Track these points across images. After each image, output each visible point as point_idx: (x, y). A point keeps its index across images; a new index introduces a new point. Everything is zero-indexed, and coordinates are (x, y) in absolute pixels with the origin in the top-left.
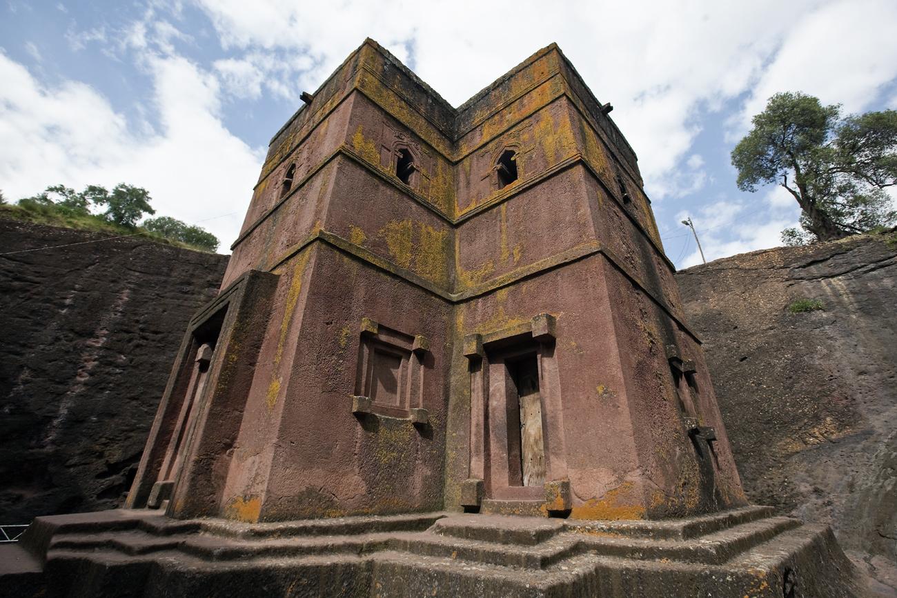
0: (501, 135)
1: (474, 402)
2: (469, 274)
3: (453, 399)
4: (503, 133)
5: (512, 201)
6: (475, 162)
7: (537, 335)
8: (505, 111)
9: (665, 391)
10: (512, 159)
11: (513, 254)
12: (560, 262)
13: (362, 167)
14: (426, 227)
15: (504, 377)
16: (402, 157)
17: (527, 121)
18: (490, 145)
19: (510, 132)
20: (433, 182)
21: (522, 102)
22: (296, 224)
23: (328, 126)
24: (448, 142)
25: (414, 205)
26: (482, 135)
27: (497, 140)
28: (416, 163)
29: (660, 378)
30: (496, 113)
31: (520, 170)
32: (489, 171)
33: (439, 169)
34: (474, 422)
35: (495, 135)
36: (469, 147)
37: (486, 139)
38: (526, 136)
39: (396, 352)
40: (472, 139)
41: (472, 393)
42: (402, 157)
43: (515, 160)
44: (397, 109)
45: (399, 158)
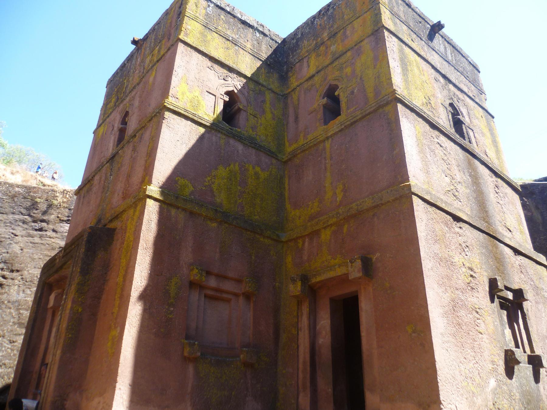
1: (301, 341)
2: (297, 212)
3: (284, 337)
7: (353, 277)
9: (483, 325)
10: (336, 93)
11: (336, 193)
13: (187, 118)
14: (254, 168)
15: (329, 315)
17: (349, 54)
18: (316, 78)
21: (345, 33)
22: (129, 176)
23: (155, 75)
25: (240, 147)
29: (477, 312)
30: (322, 44)
31: (343, 105)
34: (301, 360)
37: (312, 71)
38: (348, 70)
39: (225, 296)
41: (300, 332)
43: (339, 95)
45: (225, 101)
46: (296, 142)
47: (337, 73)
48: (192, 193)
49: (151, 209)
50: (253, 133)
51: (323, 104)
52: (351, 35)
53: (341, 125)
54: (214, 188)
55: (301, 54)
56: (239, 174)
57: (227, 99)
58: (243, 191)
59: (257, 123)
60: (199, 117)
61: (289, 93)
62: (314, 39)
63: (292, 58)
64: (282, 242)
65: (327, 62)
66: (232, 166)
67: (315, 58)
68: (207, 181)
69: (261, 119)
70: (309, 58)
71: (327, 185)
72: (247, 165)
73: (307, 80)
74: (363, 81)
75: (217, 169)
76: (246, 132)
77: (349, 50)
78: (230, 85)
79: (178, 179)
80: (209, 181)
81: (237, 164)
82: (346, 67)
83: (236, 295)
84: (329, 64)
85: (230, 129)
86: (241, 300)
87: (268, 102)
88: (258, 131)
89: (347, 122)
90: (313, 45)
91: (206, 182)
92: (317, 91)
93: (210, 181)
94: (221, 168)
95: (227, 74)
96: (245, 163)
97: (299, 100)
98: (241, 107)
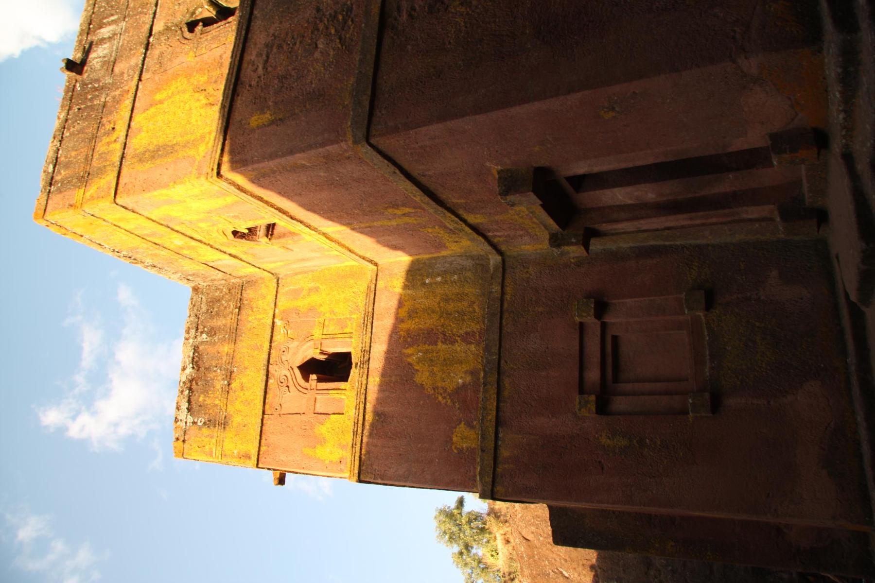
12: (403, 178)
28: (311, 352)
48: (470, 425)
49: (509, 489)
50: (350, 325)
54: (451, 387)
56: (418, 346)
57: (313, 377)
58: (442, 336)
59: (333, 319)
60: (356, 425)
64: (503, 261)
68: (445, 400)
69: (324, 313)
71: (395, 224)
75: (422, 385)
79: (456, 448)
80: (444, 398)
83: (604, 326)
85: (356, 367)
86: (609, 319)
91: (447, 402)
93: (443, 395)
94: (418, 379)
95: (279, 381)
96: (400, 338)
98: (318, 351)
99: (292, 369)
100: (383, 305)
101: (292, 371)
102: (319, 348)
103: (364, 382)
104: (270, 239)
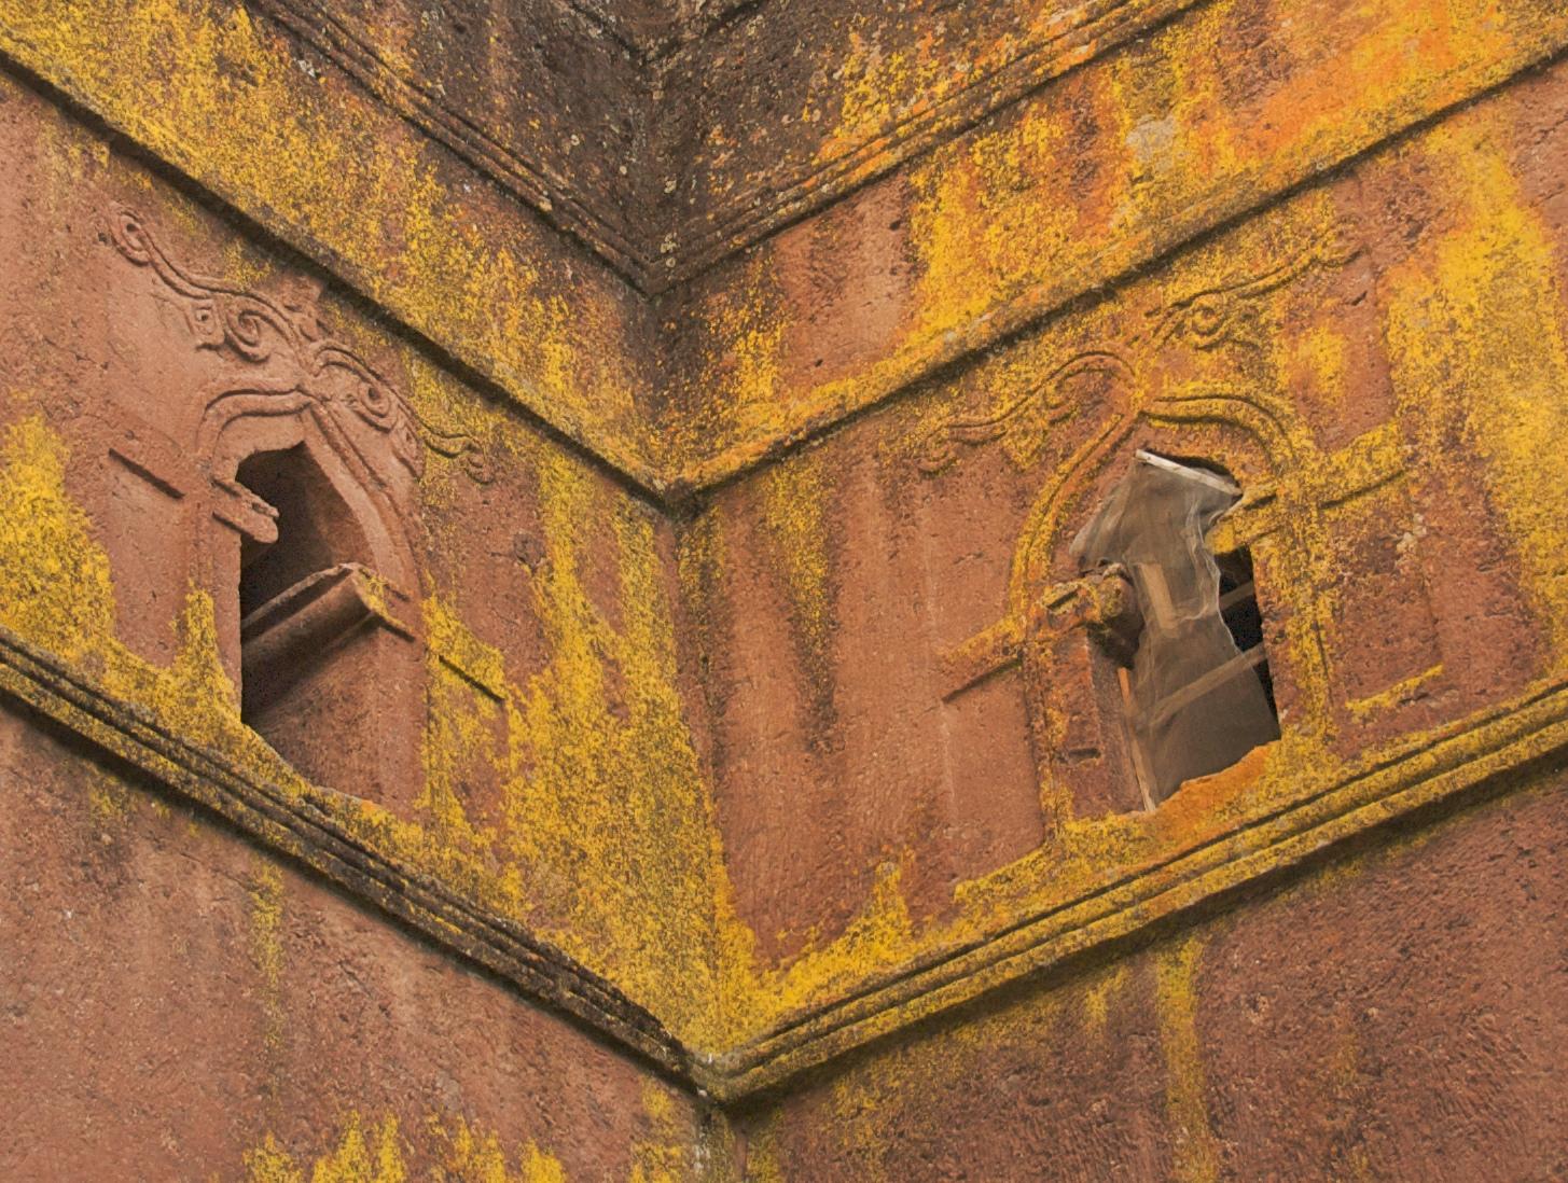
0: (1090, 300)
4: (1111, 290)
5: (1253, 933)
6: (871, 521)
8: (1112, 88)
16: (267, 532)
17: (1315, 210)
19: (1175, 289)
20: (531, 727)
24: (605, 307)
26: (917, 268)
27: (1054, 349)
32: (1012, 627)
33: (565, 580)
35: (1038, 297)
36: (797, 371)
40: (831, 285)
42: (266, 530)
44: (200, 88)
45: (249, 544)
46: (839, 933)
47: (1205, 359)
50: (479, 840)
51: (1095, 614)
52: (1319, 55)
53: (1303, 827)
55: (829, 150)
59: (502, 750)
61: (733, 479)
62: (951, 38)
63: (733, 170)
65: (1119, 257)
66: (353, 1141)
67: (966, 201)
69: (522, 708)
70: (911, 194)
72: (464, 1143)
73: (911, 391)
74: (1476, 460)
76: (428, 827)
77: (1314, 181)
78: (273, 403)
81: (392, 1124)
82: (1296, 323)
84: (1127, 279)
87: (564, 563)
88: (510, 823)
89: (1356, 804)
90: (941, 88)
92: (1022, 499)
95: (253, 305)
97: (832, 549)
98: (374, 603)
99: (297, 412)
100: (576, 1074)
101: (290, 402)
102: (387, 617)
103: (275, 832)
104: (1093, 628)
